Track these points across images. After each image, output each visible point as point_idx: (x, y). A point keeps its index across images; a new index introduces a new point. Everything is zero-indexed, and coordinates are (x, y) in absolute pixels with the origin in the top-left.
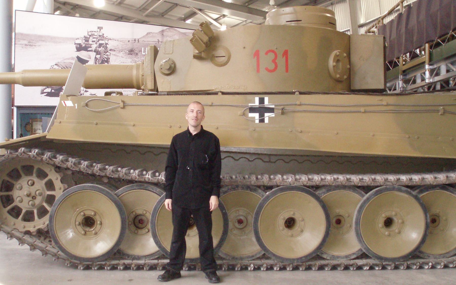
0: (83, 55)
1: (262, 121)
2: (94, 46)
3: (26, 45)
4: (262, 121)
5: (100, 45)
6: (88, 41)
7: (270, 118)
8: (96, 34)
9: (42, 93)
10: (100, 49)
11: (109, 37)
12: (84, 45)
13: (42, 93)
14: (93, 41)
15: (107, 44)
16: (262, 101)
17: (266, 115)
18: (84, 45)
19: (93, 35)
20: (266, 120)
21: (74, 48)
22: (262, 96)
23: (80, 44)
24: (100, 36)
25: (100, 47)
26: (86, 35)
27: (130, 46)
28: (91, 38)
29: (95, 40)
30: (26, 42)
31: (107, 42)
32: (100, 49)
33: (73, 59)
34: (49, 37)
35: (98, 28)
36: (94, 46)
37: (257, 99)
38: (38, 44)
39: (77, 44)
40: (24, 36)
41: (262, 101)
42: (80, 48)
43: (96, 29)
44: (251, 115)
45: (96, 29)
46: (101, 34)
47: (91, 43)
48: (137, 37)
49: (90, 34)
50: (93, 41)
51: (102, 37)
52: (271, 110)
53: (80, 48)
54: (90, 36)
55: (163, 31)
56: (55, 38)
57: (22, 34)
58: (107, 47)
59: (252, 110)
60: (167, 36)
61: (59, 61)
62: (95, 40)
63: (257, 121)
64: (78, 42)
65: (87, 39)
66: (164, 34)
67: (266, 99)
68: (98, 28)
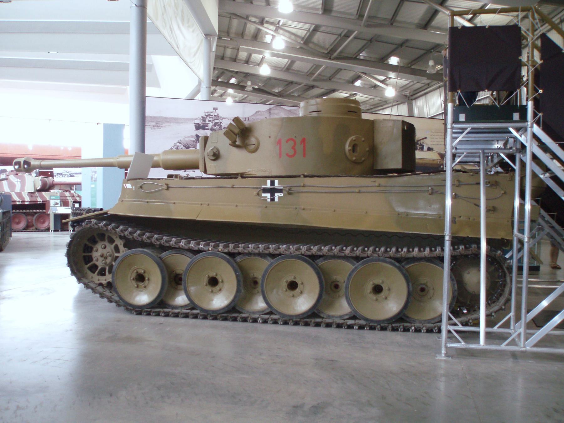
0: (202, 133)
2: (210, 125)
3: (154, 126)
5: (216, 124)
8: (212, 114)
10: (215, 128)
11: (224, 116)
12: (201, 125)
14: (209, 121)
15: (221, 123)
18: (201, 125)
19: (209, 115)
21: (193, 127)
23: (198, 124)
24: (215, 116)
25: (215, 126)
26: (204, 115)
28: (208, 118)
29: (211, 119)
30: (154, 124)
31: (221, 121)
32: (215, 128)
33: (192, 136)
34: (172, 118)
35: (214, 109)
36: (210, 125)
38: (164, 125)
39: (196, 124)
40: (153, 118)
42: (198, 127)
43: (212, 110)
45: (212, 110)
46: (216, 114)
47: (207, 122)
49: (207, 114)
50: (209, 121)
51: (217, 117)
53: (198, 127)
54: (207, 116)
55: (270, 109)
56: (177, 119)
57: (150, 117)
58: (221, 126)
60: (274, 114)
61: (181, 139)
62: (211, 119)
64: (197, 121)
65: (204, 119)
66: (271, 112)
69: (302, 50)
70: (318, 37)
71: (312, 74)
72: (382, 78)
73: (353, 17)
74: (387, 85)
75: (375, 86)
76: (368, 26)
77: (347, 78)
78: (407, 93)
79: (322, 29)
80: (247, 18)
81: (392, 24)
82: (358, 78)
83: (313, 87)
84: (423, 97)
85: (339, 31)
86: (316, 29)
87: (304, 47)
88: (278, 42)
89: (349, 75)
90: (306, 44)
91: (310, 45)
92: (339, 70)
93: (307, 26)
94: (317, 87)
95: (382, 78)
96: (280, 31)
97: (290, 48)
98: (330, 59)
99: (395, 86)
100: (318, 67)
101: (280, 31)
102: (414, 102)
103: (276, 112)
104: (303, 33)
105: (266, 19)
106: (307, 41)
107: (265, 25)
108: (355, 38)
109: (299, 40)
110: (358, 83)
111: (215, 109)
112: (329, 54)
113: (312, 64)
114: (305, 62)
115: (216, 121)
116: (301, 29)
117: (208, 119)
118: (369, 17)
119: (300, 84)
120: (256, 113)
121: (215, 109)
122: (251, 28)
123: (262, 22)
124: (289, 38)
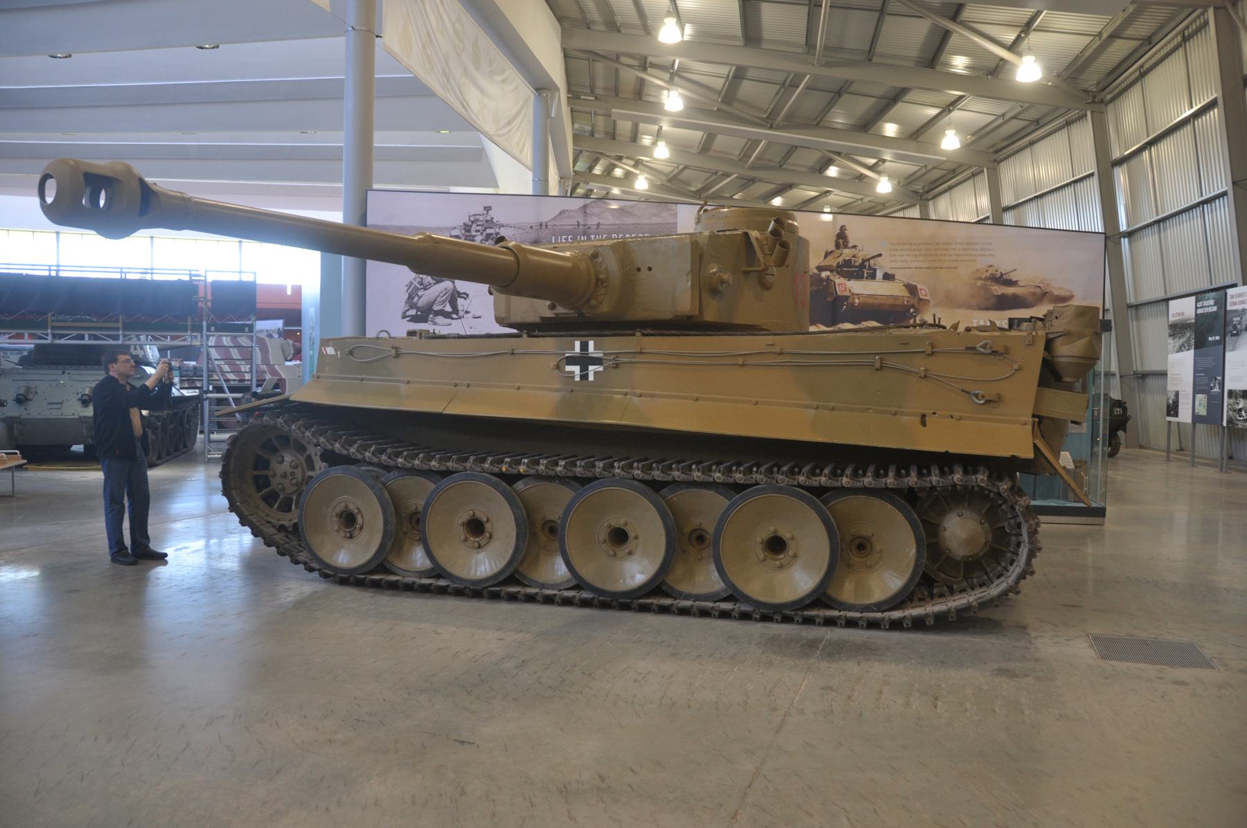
1: (584, 377)
4: (584, 377)
5: (488, 237)
6: (469, 231)
7: (596, 373)
9: (404, 317)
11: (503, 221)
13: (404, 317)
16: (584, 346)
17: (591, 368)
20: (591, 378)
22: (585, 339)
25: (487, 240)
27: (532, 236)
35: (485, 208)
36: (479, 238)
37: (577, 344)
41: (584, 346)
43: (481, 210)
44: (568, 368)
45: (481, 210)
48: (545, 219)
51: (490, 223)
52: (597, 361)
55: (585, 206)
59: (572, 361)
63: (577, 379)
64: (454, 233)
65: (467, 228)
67: (591, 344)
68: (485, 208)
69: (720, 114)
70: (747, 89)
71: (747, 156)
72: (872, 161)
73: (801, 50)
74: (879, 173)
75: (861, 177)
76: (828, 65)
77: (811, 164)
78: (918, 187)
79: (750, 74)
80: (617, 58)
81: (870, 60)
82: (829, 162)
83: (753, 181)
84: (947, 195)
85: (780, 78)
86: (739, 75)
87: (724, 107)
88: (673, 101)
89: (812, 158)
90: (724, 103)
91: (736, 104)
92: (793, 149)
93: (724, 70)
94: (761, 180)
95: (872, 161)
96: (676, 79)
97: (695, 108)
98: (771, 128)
99: (891, 176)
100: (756, 142)
101: (676, 79)
102: (931, 203)
103: (596, 210)
104: (719, 83)
105: (650, 59)
106: (729, 95)
107: (649, 70)
108: (808, 88)
109: (715, 97)
110: (832, 172)
111: (488, 209)
112: (769, 121)
113: (745, 141)
114: (731, 138)
115: (489, 231)
116: (714, 74)
117: (474, 227)
118: (826, 48)
119: (727, 175)
120: (561, 213)
121: (488, 209)
122: (629, 76)
123: (644, 65)
124: (689, 90)
